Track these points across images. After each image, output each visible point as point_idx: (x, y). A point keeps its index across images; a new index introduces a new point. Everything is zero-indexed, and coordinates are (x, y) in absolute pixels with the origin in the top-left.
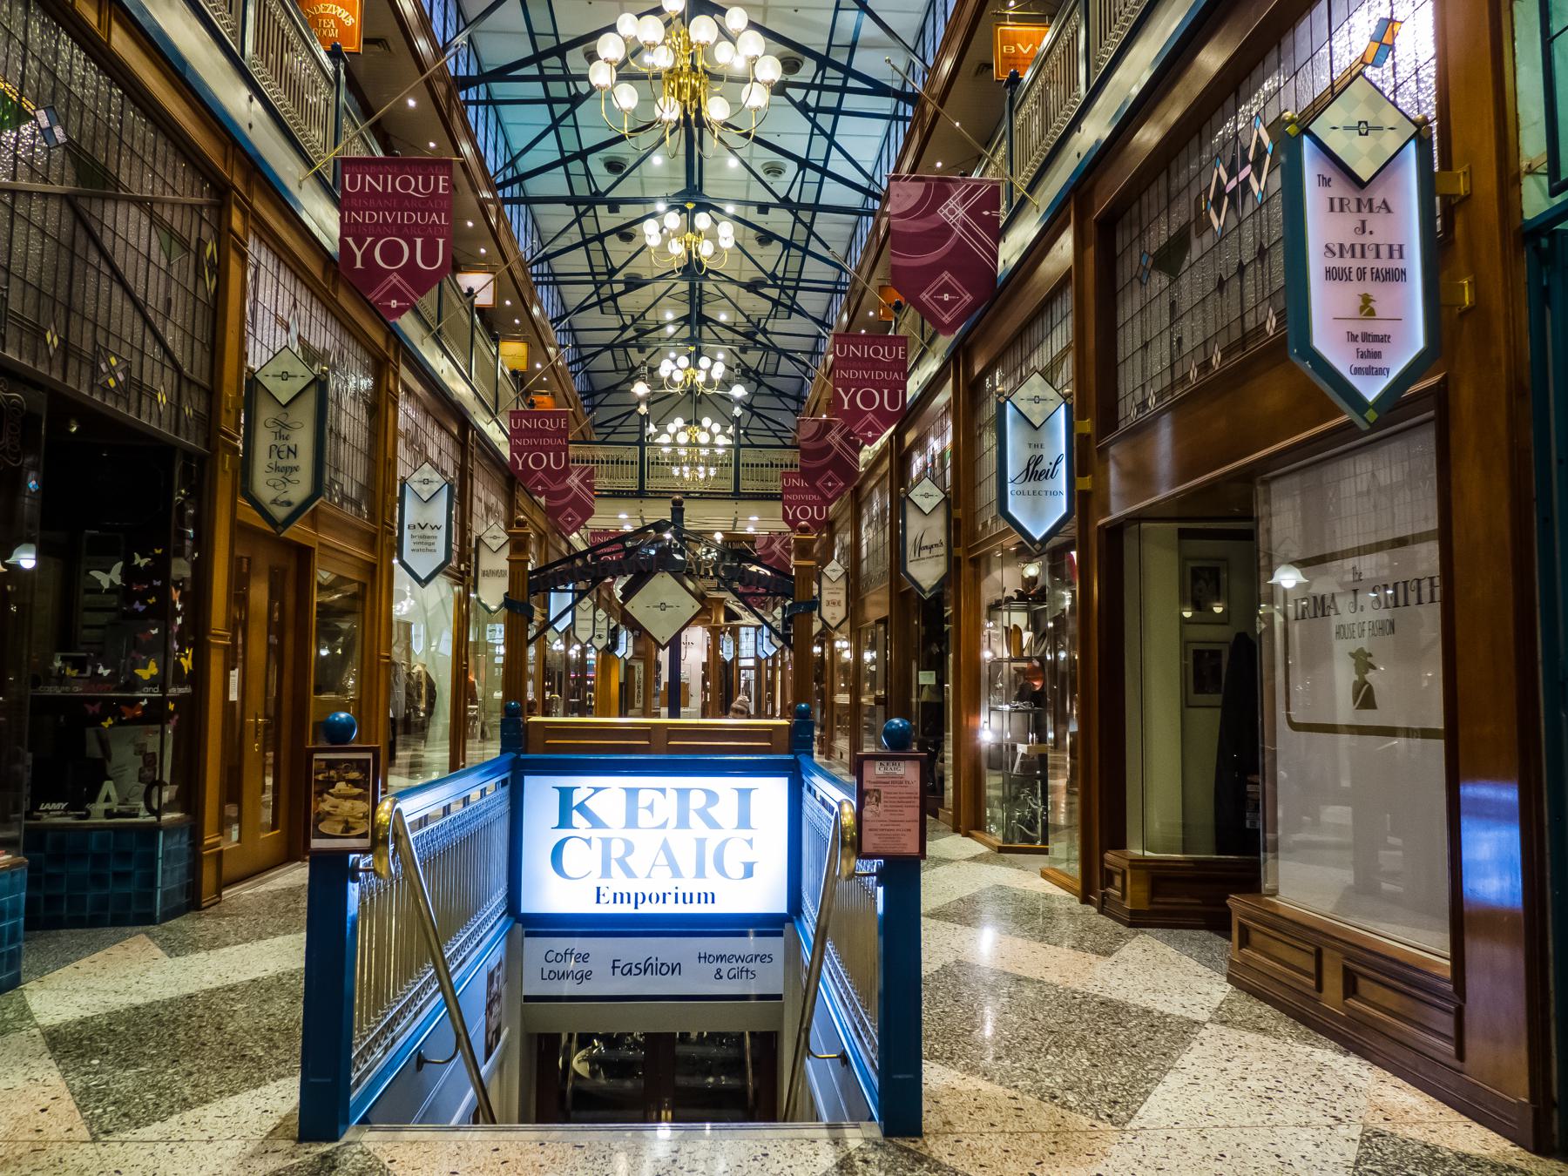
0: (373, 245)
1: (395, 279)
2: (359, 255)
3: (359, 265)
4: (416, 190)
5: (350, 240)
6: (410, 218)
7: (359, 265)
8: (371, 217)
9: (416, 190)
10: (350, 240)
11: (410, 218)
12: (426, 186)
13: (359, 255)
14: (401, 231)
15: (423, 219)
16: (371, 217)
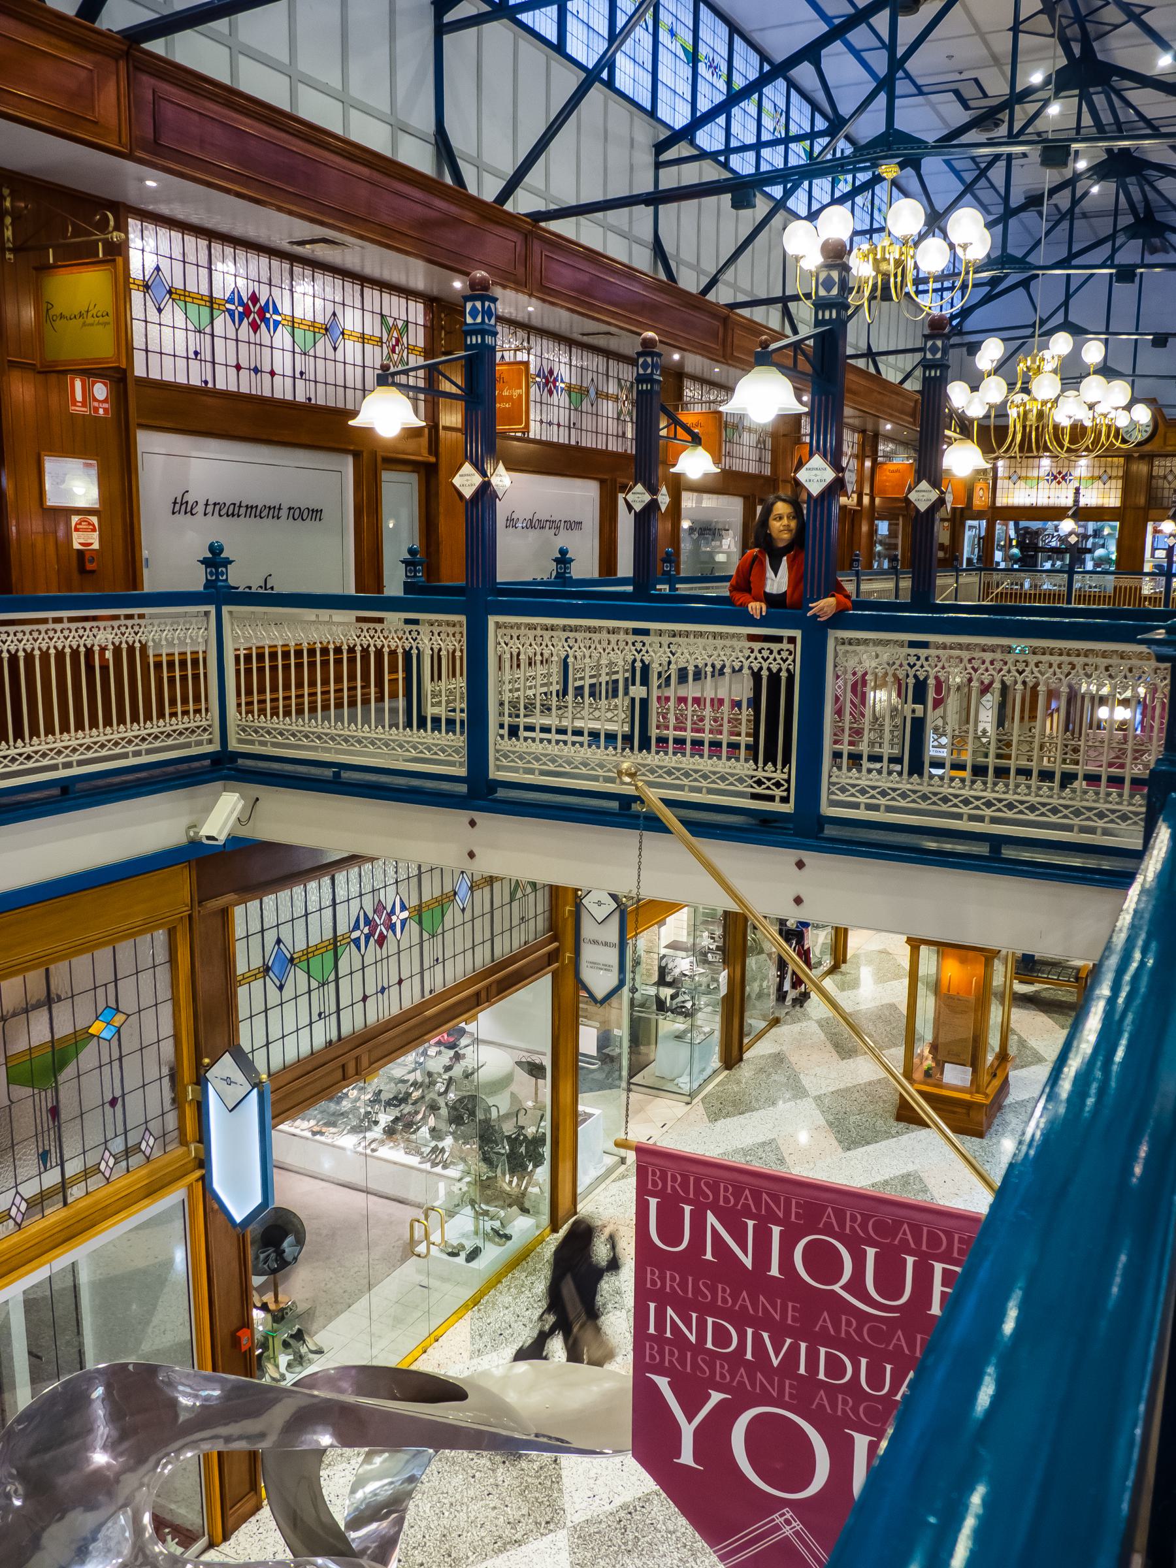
0: (724, 1417)
1: (788, 1526)
2: (688, 1431)
3: (687, 1457)
4: (856, 1285)
5: (662, 1383)
6: (836, 1369)
7: (687, 1457)
8: (722, 1337)
9: (856, 1285)
10: (662, 1383)
11: (836, 1369)
12: (889, 1281)
13: (688, 1431)
14: (805, 1395)
15: (875, 1379)
16: (722, 1337)
